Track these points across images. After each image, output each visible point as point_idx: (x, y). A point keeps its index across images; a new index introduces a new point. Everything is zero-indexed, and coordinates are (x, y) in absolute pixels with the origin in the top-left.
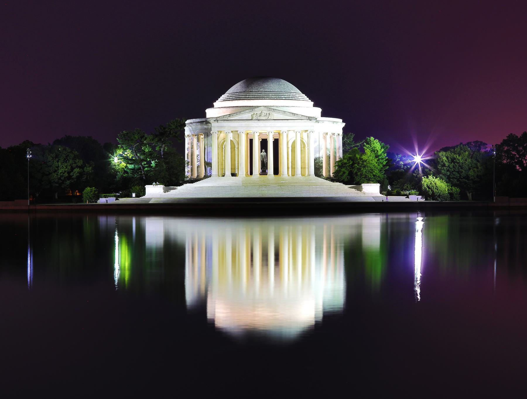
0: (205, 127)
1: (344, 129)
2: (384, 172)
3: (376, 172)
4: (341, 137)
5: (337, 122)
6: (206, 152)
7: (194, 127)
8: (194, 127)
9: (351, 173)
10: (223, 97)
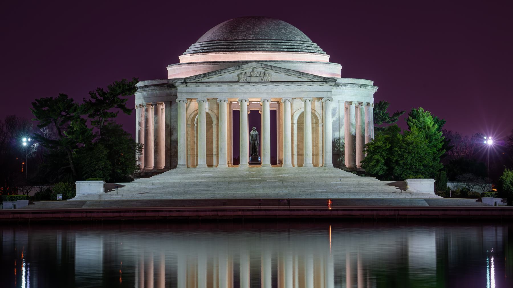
0: (168, 91)
1: (375, 95)
2: (439, 160)
3: (428, 160)
4: (372, 108)
5: (366, 86)
6: (171, 130)
7: (150, 92)
8: (150, 92)
9: (388, 162)
10: (195, 46)
